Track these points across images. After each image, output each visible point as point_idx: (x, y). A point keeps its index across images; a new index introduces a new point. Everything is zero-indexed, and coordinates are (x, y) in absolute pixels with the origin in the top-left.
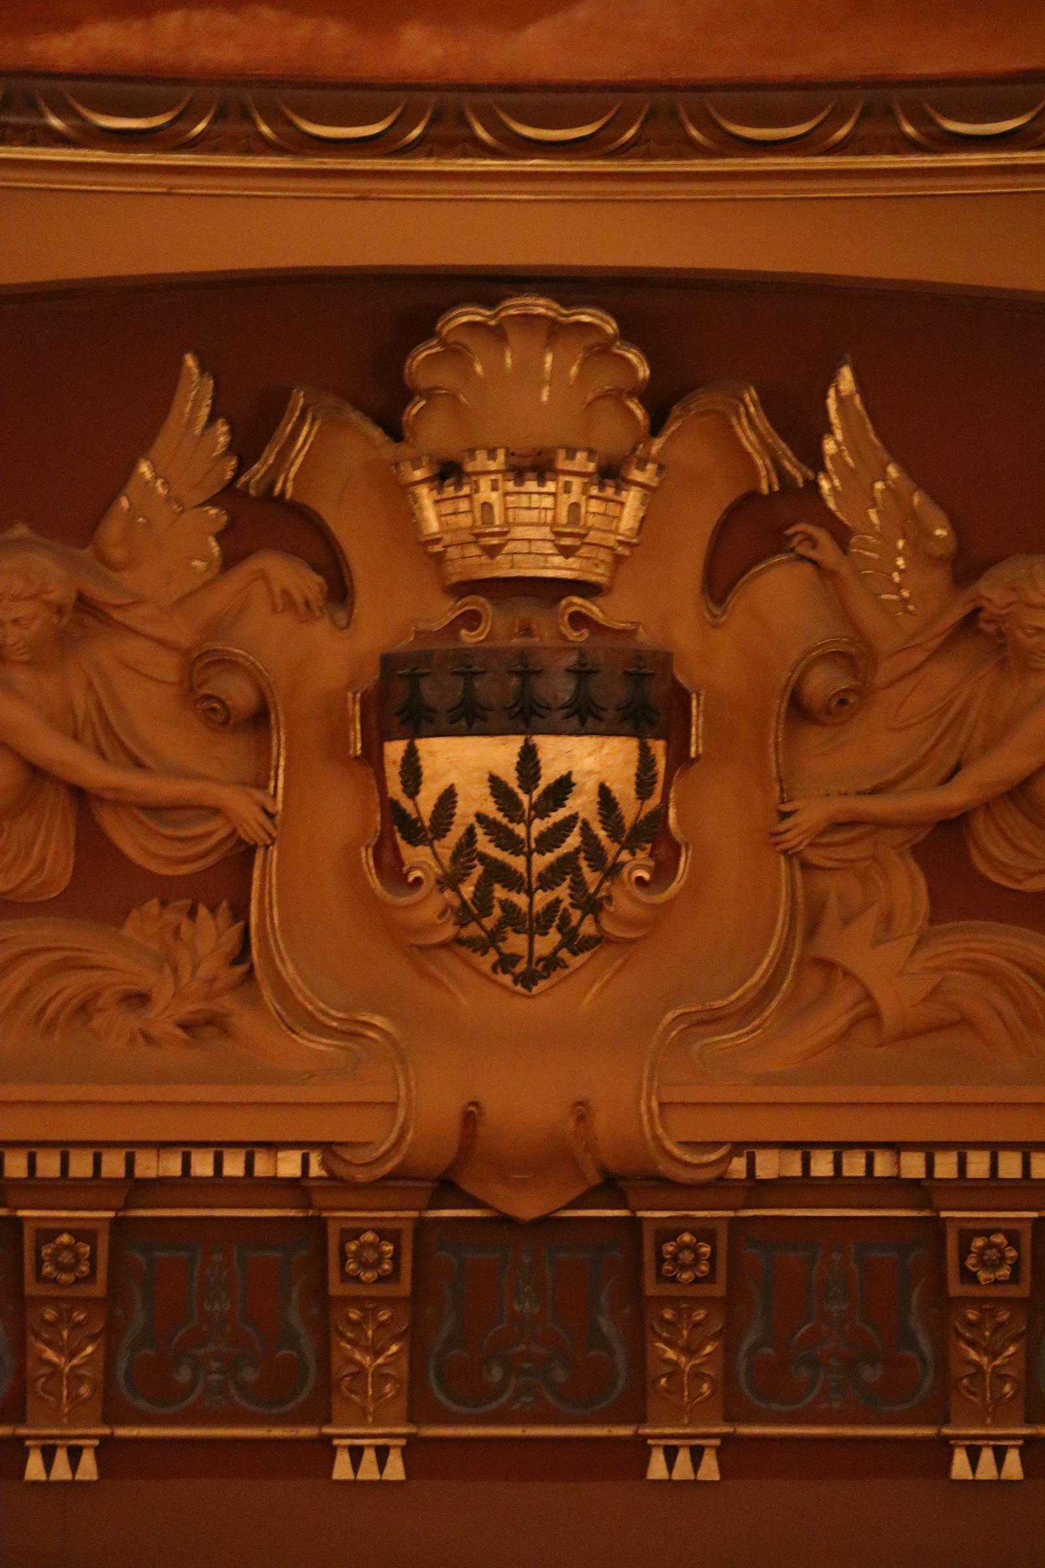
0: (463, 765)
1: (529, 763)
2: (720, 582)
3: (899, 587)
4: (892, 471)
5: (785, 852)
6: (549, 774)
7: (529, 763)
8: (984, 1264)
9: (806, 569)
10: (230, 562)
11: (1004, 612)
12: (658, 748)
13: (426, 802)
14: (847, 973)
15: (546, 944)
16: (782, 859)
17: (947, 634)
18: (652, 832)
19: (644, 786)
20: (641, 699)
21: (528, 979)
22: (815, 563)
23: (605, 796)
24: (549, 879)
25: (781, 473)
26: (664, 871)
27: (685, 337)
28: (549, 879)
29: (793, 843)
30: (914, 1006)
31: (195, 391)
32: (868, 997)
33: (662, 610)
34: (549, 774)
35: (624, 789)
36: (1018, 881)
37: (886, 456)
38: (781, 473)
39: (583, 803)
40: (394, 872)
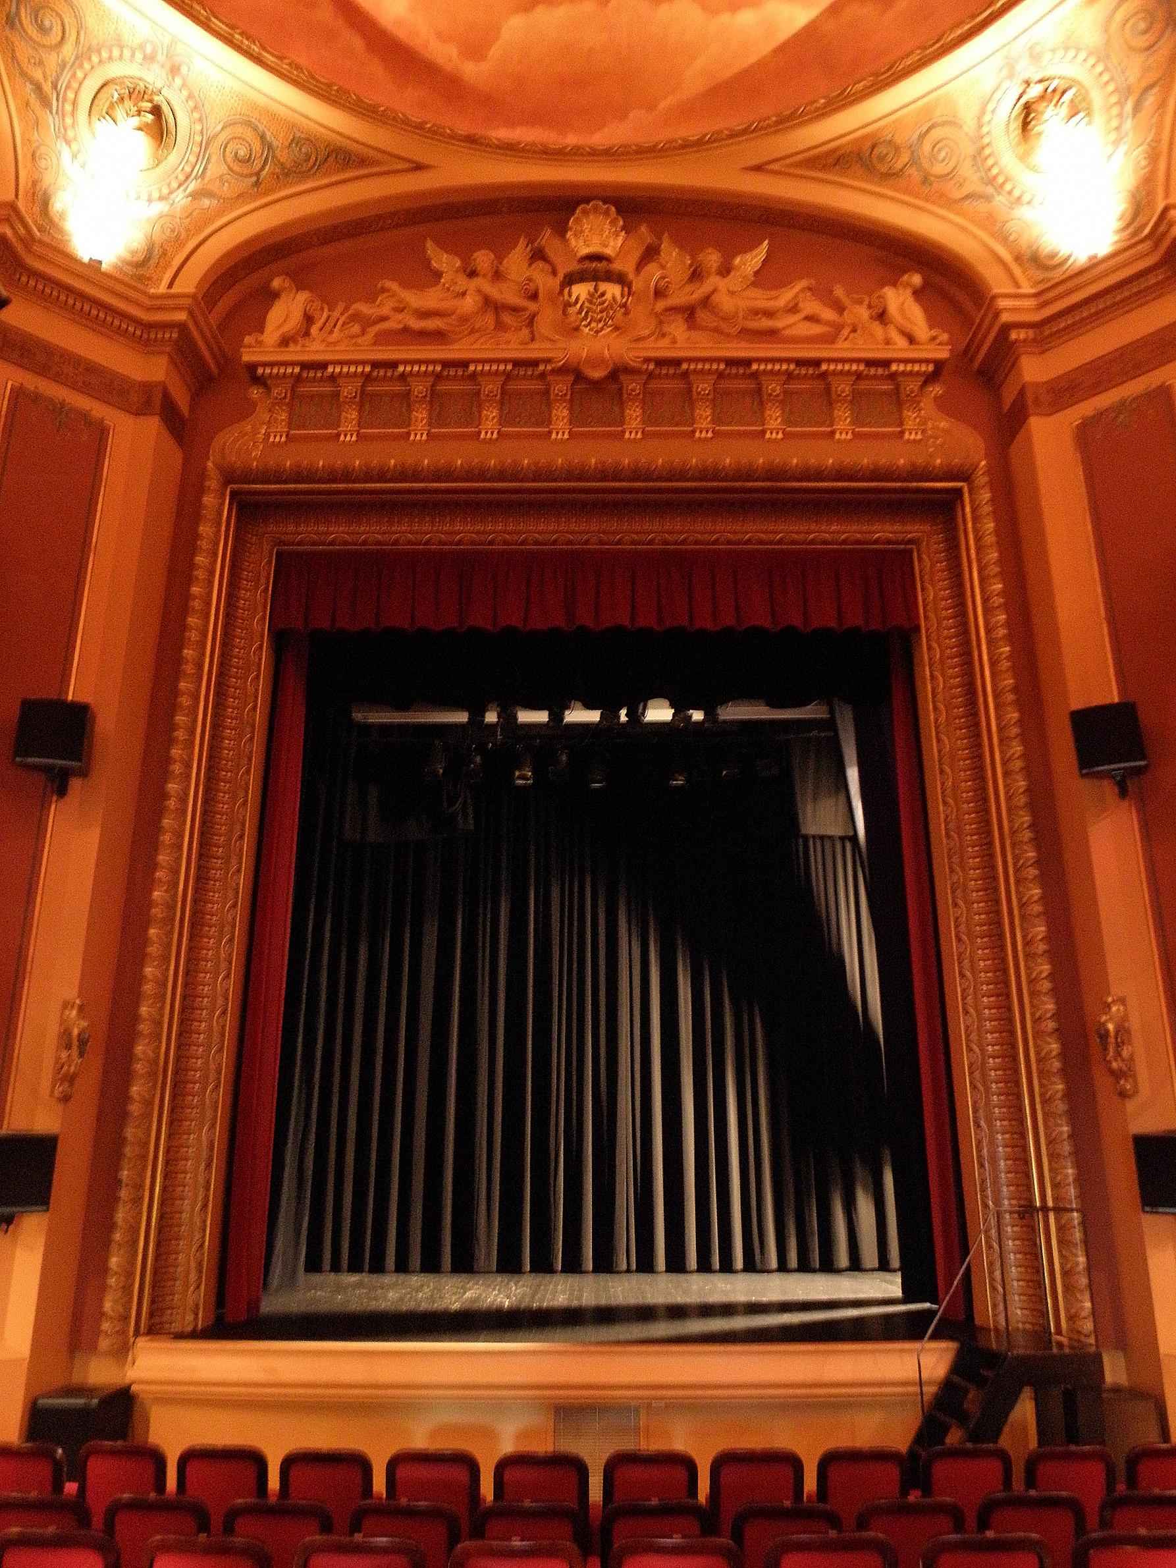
0: (581, 291)
1: (596, 289)
2: (639, 267)
6: (601, 290)
7: (596, 289)
10: (530, 265)
12: (626, 289)
13: (574, 298)
15: (600, 325)
18: (624, 305)
19: (622, 296)
20: (620, 279)
21: (597, 332)
23: (614, 298)
24: (602, 312)
26: (626, 313)
27: (632, 207)
28: (602, 312)
31: (522, 242)
33: (626, 265)
34: (601, 290)
35: (618, 297)
39: (608, 296)
40: (565, 313)
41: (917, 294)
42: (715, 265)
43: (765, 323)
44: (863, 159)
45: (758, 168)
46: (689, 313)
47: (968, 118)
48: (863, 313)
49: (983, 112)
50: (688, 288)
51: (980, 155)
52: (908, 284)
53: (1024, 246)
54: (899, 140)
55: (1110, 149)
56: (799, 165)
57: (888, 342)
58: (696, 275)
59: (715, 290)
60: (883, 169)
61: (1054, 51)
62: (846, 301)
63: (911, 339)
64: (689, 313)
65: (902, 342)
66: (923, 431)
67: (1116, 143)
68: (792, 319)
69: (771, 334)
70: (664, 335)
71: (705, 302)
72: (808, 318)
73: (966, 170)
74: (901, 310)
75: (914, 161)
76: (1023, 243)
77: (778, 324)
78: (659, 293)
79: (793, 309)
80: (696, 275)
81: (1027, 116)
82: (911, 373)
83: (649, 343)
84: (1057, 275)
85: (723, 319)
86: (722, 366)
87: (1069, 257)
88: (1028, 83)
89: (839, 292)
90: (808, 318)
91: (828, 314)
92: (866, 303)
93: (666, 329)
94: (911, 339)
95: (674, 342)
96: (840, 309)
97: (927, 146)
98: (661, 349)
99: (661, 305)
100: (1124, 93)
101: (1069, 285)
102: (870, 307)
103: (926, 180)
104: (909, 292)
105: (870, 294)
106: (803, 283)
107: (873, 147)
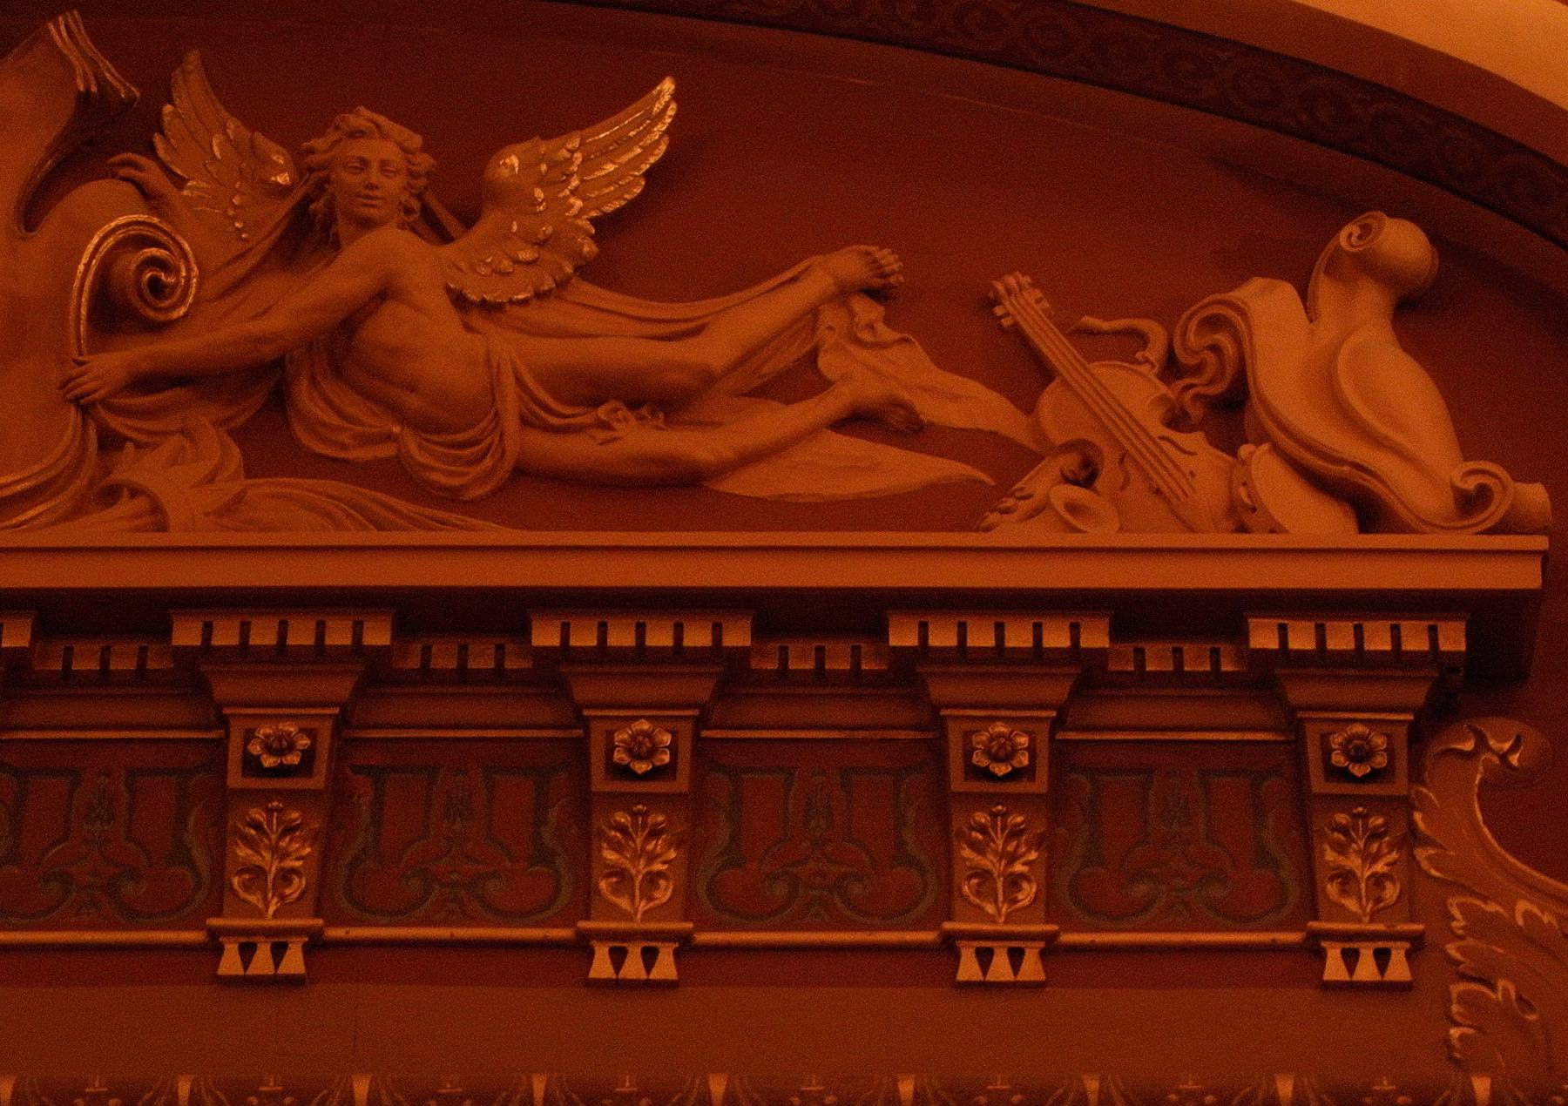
3: (234, 219)
4: (232, 124)
5: (76, 400)
8: (269, 749)
9: (128, 188)
11: (327, 156)
14: (135, 492)
16: (73, 409)
17: (277, 233)
22: (138, 185)
25: (100, 80)
29: (86, 387)
30: (207, 514)
32: (156, 508)
36: (344, 447)
37: (226, 114)
38: (100, 80)
41: (1415, 311)
42: (393, 185)
43: (639, 439)
46: (257, 397)
48: (1136, 392)
50: (271, 286)
52: (1368, 266)
57: (1241, 515)
58: (308, 231)
59: (384, 294)
62: (1054, 347)
63: (1369, 511)
64: (257, 397)
65: (1322, 521)
66: (1416, 946)
68: (771, 422)
69: (677, 489)
70: (111, 495)
71: (341, 342)
72: (858, 421)
74: (1325, 386)
77: (695, 445)
78: (113, 312)
79: (800, 381)
80: (308, 231)
82: (1360, 662)
83: (37, 524)
85: (423, 425)
86: (378, 635)
89: (1025, 304)
90: (858, 421)
91: (970, 404)
92: (1155, 352)
93: (128, 469)
94: (1369, 511)
95: (157, 517)
96: (1025, 372)
98: (92, 553)
99: (112, 364)
102: (1171, 368)
104: (1371, 302)
105: (1168, 314)
106: (849, 264)
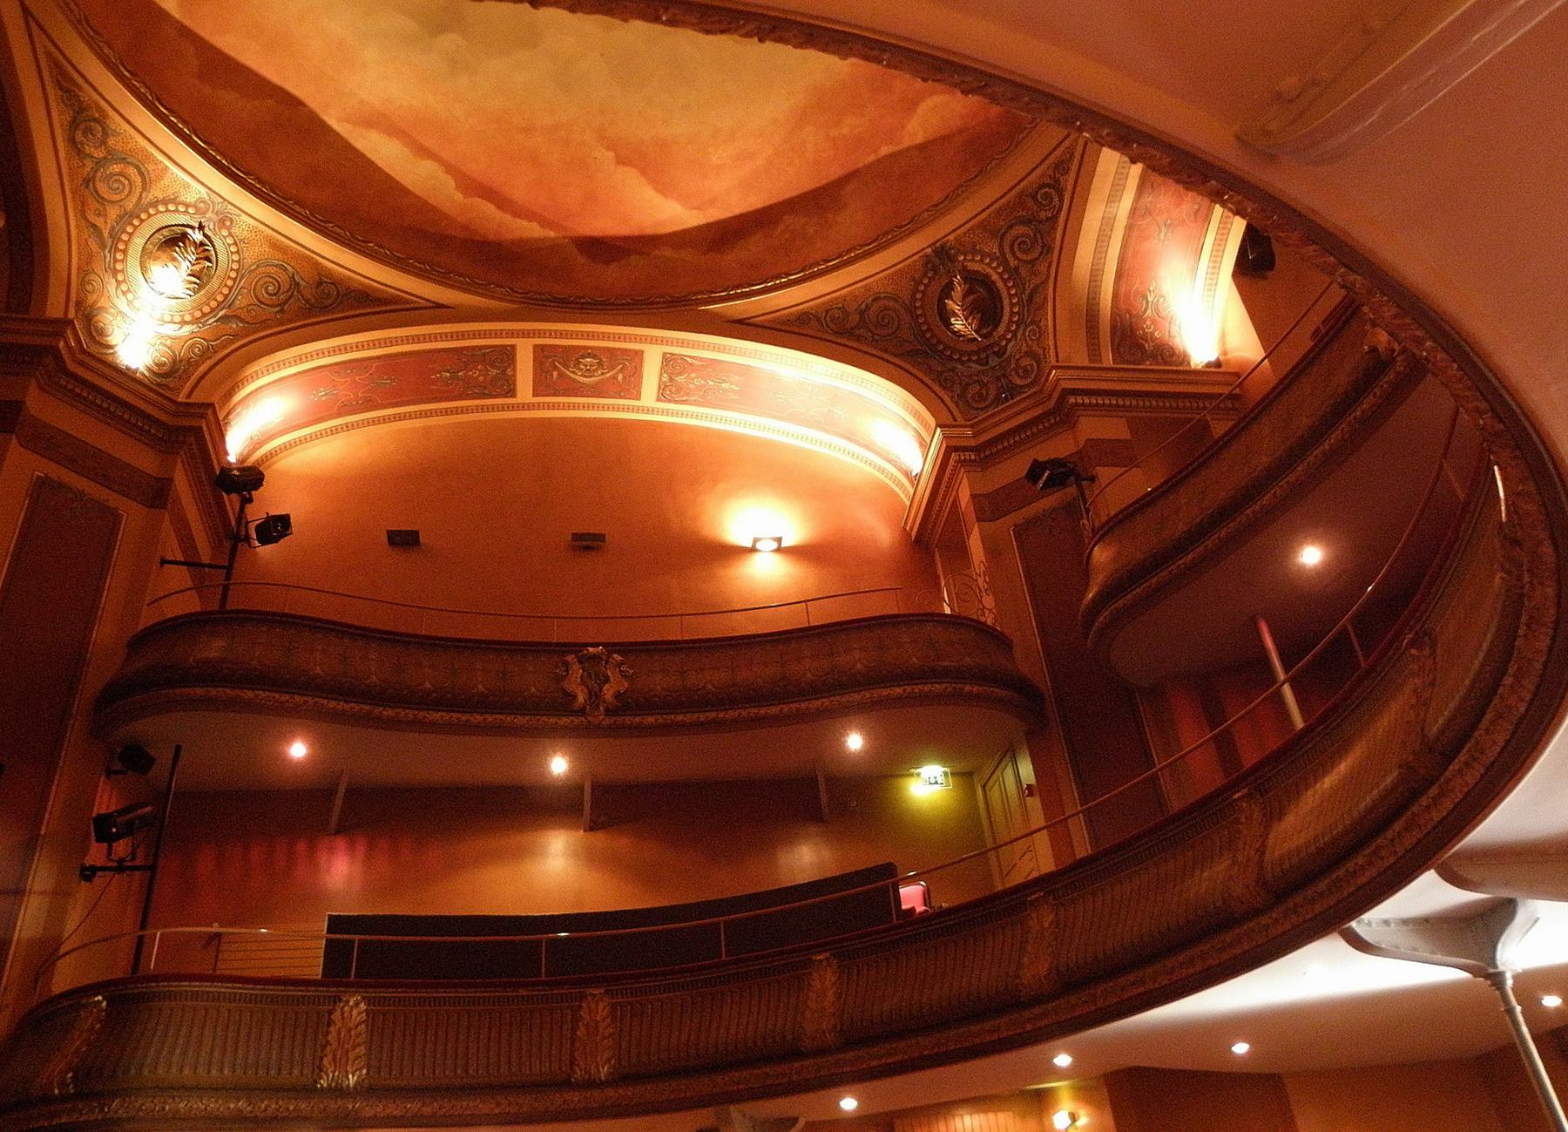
44: (85, 120)
45: (26, 12)
47: (156, 192)
49: (165, 202)
51: (129, 217)
53: (90, 302)
54: (111, 142)
55: (188, 318)
56: (49, 55)
60: (79, 136)
61: (230, 235)
67: (195, 321)
73: (113, 212)
75: (100, 163)
76: (91, 299)
81: (174, 240)
84: (93, 349)
87: (111, 347)
88: (201, 227)
97: (116, 168)
100: (226, 302)
101: (93, 363)
103: (88, 181)
107: (96, 120)
